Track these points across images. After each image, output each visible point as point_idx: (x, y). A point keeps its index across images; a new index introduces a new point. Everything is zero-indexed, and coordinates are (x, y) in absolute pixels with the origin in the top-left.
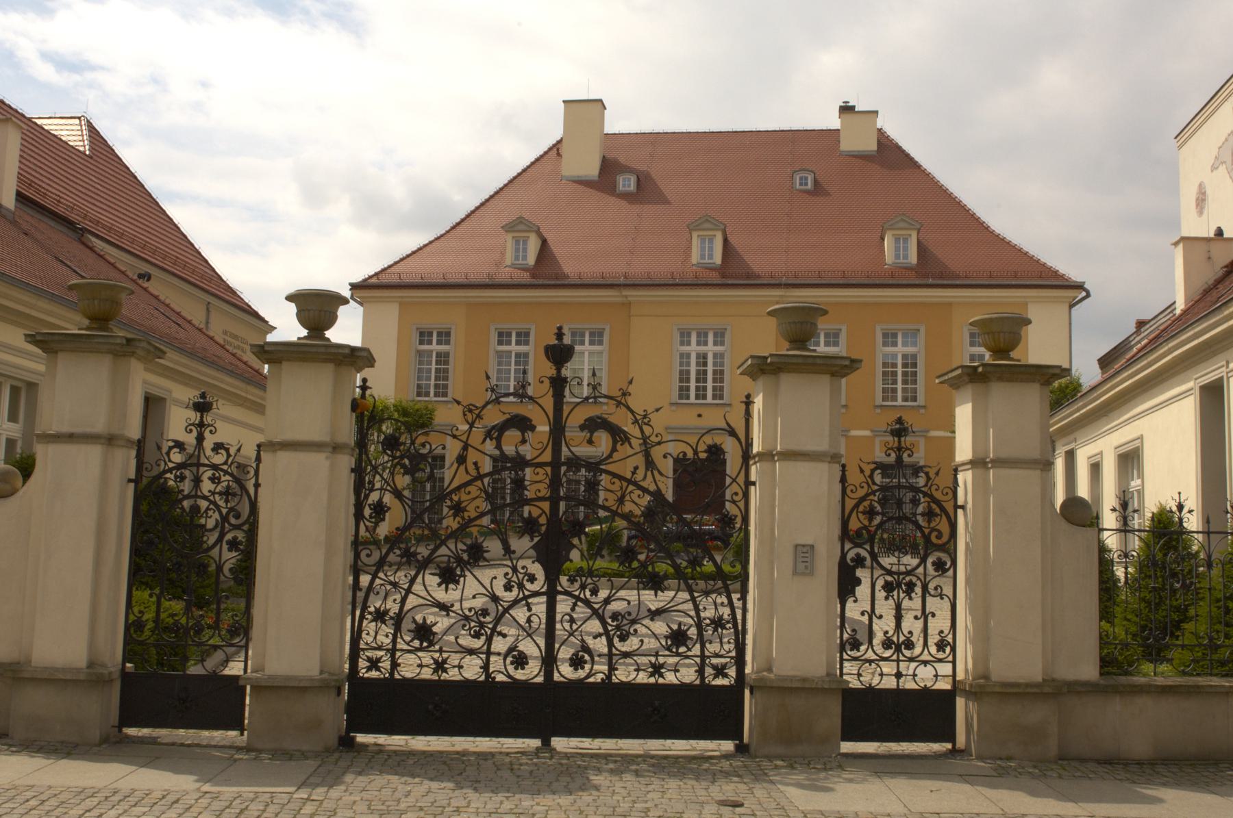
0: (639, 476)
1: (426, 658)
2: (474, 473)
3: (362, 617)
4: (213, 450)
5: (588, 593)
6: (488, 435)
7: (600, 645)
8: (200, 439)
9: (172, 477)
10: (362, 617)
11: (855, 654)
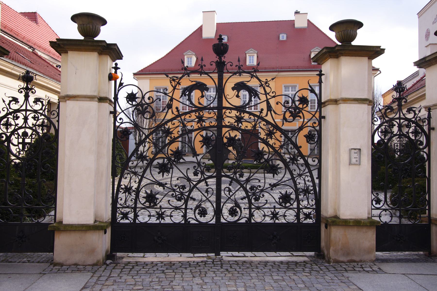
0: (264, 114)
1: (153, 212)
2: (176, 113)
3: (118, 191)
4: (34, 102)
5: (238, 176)
6: (184, 93)
7: (244, 204)
8: (27, 97)
9: (12, 117)
10: (118, 191)
11: (378, 206)
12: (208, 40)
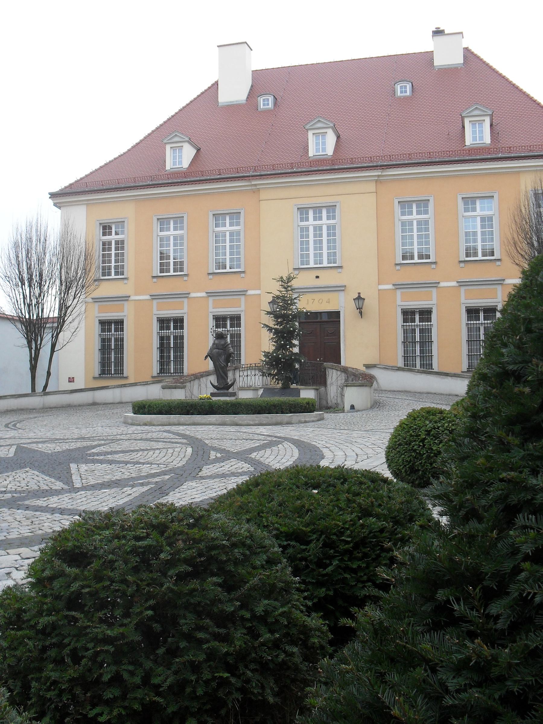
12: (233, 108)
